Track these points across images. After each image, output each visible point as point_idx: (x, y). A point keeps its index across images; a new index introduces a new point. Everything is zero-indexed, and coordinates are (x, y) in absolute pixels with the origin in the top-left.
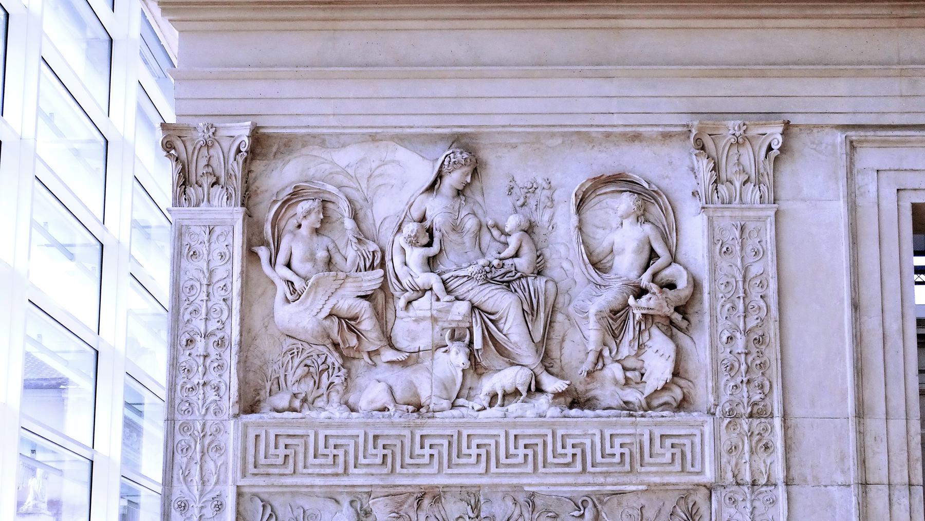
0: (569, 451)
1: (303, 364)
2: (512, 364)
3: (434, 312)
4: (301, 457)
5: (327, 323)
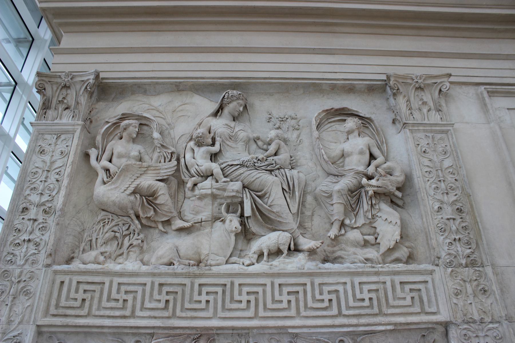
0: (326, 297)
1: (111, 230)
2: (275, 230)
3: (214, 190)
4: (96, 301)
5: (132, 198)
